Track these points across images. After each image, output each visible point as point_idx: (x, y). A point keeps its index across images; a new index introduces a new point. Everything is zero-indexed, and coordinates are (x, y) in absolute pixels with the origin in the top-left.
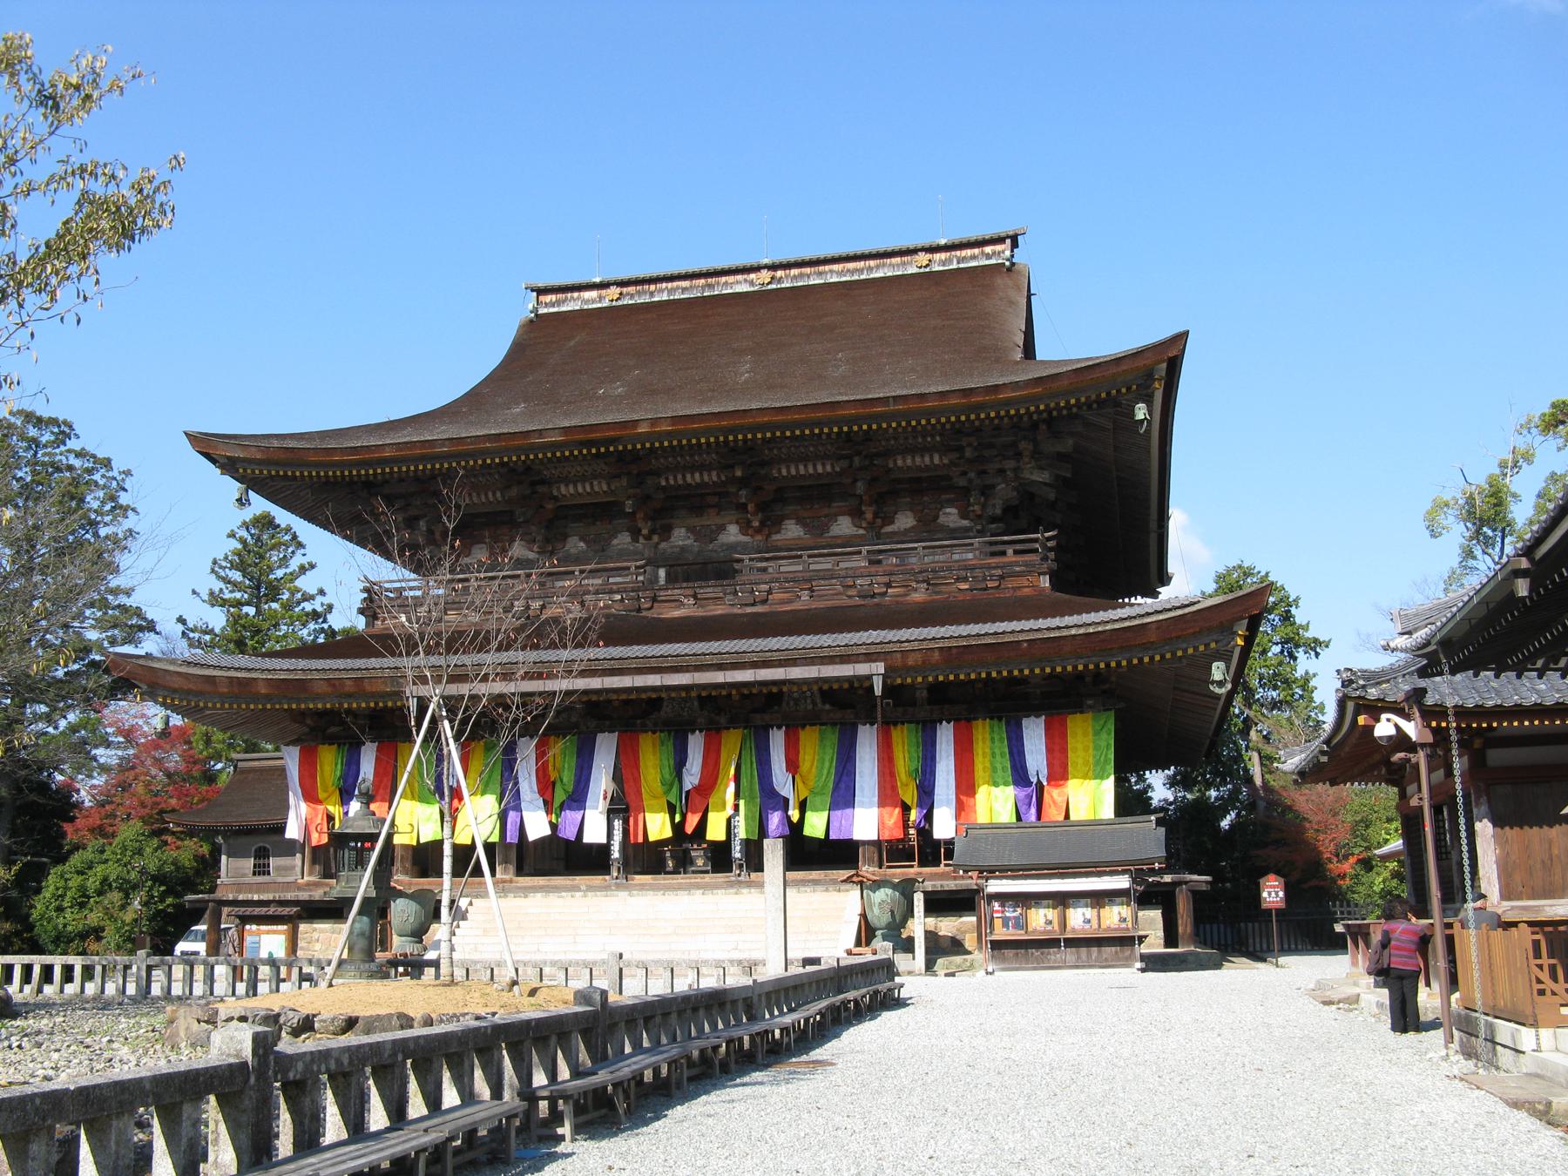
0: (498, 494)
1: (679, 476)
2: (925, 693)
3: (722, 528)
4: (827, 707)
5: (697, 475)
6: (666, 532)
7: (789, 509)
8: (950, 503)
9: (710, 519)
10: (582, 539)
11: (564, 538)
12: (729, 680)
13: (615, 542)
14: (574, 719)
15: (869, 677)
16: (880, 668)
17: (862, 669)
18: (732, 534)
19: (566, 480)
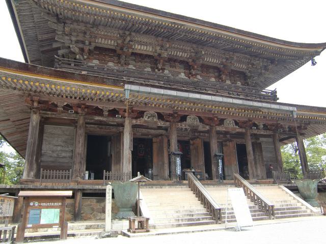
0: (113, 42)
1: (176, 52)
2: (262, 126)
3: (180, 73)
4: (237, 127)
5: (181, 53)
6: (163, 69)
7: (199, 72)
8: (239, 81)
9: (177, 70)
10: (135, 66)
11: (129, 64)
12: (254, 105)
13: (145, 70)
14: (155, 120)
15: (292, 112)
16: (295, 109)
17: (291, 108)
18: (183, 76)
19: (140, 43)
